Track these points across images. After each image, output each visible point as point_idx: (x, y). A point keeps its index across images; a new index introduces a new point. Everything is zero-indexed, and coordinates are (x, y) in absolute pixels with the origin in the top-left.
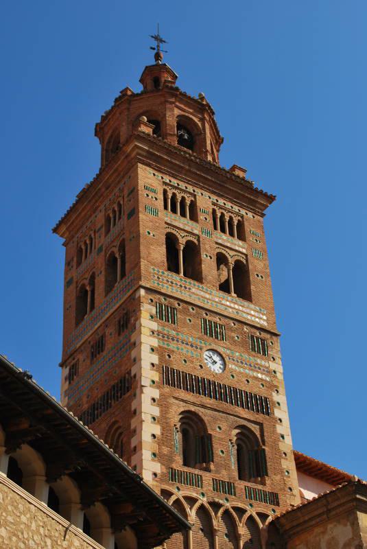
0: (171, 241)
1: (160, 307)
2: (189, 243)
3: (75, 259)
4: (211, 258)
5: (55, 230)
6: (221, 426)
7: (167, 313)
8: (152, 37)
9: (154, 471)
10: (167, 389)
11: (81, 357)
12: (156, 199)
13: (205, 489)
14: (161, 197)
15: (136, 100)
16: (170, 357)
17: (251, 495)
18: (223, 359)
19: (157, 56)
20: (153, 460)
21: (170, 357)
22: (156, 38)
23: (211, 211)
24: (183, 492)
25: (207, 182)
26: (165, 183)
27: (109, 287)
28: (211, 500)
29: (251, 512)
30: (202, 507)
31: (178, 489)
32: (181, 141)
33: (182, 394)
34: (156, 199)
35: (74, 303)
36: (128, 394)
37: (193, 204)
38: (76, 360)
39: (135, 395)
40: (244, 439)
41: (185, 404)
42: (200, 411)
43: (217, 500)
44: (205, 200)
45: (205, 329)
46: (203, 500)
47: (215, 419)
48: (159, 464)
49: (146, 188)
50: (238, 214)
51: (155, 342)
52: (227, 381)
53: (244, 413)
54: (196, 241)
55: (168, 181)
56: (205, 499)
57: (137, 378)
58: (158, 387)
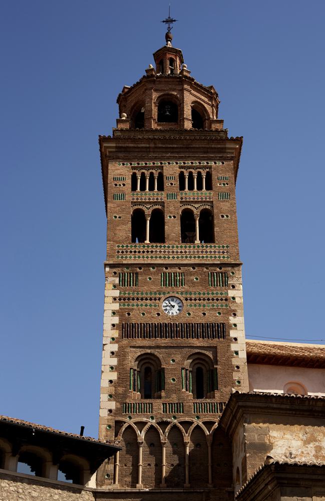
4: (174, 217)
6: (175, 358)
8: (164, 22)
9: (109, 408)
10: (125, 342)
12: (124, 185)
13: (154, 413)
14: (129, 181)
15: (128, 97)
16: (129, 314)
17: (198, 409)
20: (109, 400)
21: (129, 314)
23: (178, 175)
24: (135, 419)
25: (174, 150)
26: (133, 168)
28: (160, 420)
30: (152, 427)
31: (130, 418)
32: (161, 118)
33: (140, 342)
34: (124, 185)
37: (161, 176)
40: (201, 362)
41: (141, 350)
42: (156, 352)
43: (165, 419)
45: (165, 281)
46: (153, 422)
47: (169, 354)
48: (115, 402)
51: (116, 306)
52: (183, 321)
53: (196, 342)
54: (160, 207)
55: (136, 165)
56: (154, 421)
58: (117, 342)
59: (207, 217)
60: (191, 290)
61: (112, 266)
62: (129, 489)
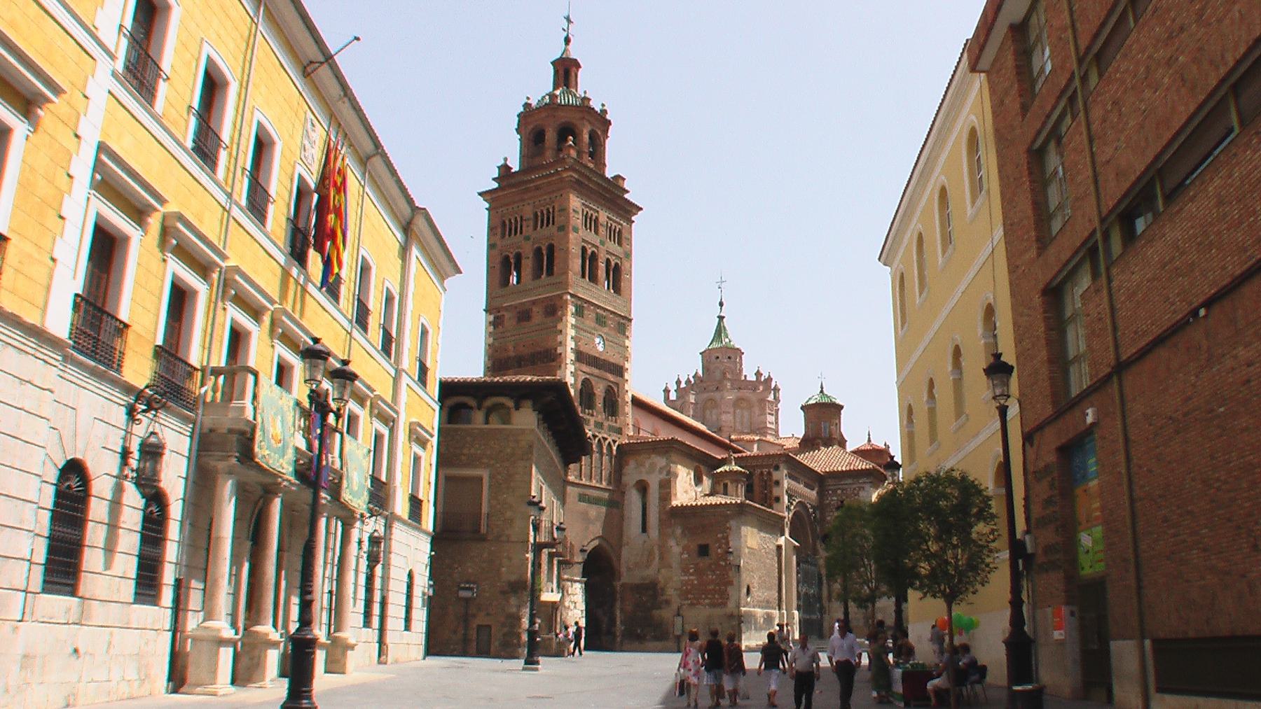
0: (584, 250)
1: (576, 306)
2: (593, 252)
3: (499, 230)
5: (480, 194)
7: (579, 313)
10: (578, 364)
11: (507, 315)
17: (611, 429)
18: (604, 341)
19: (567, 41)
22: (568, 20)
26: (583, 204)
27: (537, 275)
29: (610, 440)
35: (498, 267)
36: (554, 364)
37: (597, 218)
38: (499, 314)
39: (560, 366)
42: (592, 378)
44: (603, 216)
49: (574, 210)
50: (619, 224)
53: (611, 377)
57: (563, 355)
58: (573, 364)
59: (617, 269)
60: (609, 332)
61: (572, 295)
62: (577, 481)
